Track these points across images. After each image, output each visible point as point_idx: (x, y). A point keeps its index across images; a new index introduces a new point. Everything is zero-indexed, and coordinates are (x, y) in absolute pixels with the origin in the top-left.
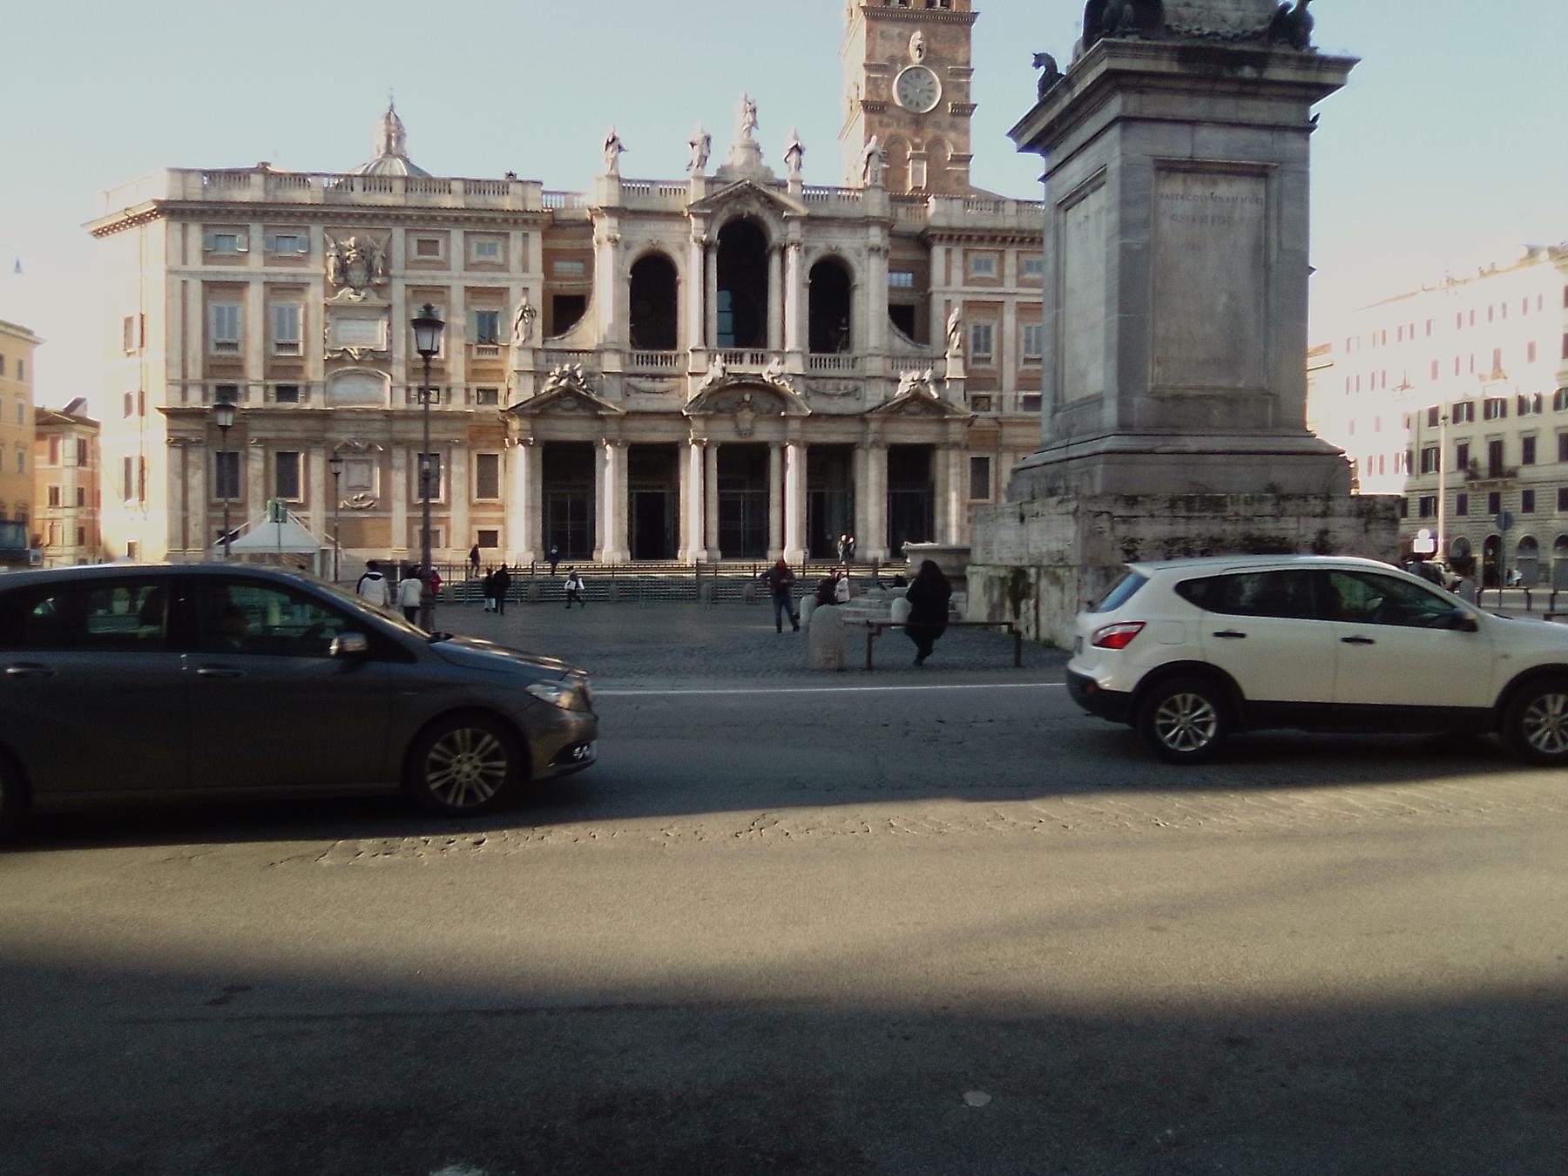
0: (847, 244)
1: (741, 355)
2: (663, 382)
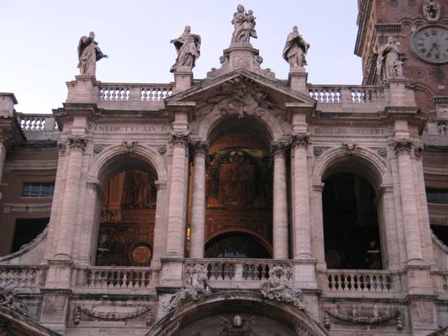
0: (367, 144)
1: (232, 265)
2: (125, 306)
